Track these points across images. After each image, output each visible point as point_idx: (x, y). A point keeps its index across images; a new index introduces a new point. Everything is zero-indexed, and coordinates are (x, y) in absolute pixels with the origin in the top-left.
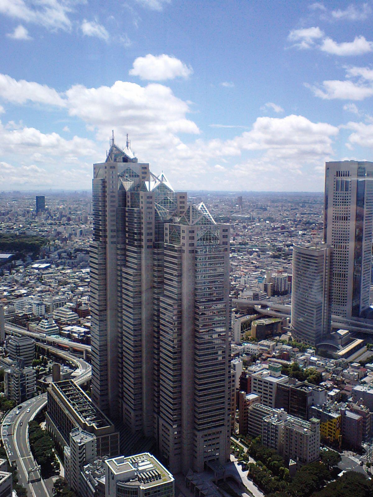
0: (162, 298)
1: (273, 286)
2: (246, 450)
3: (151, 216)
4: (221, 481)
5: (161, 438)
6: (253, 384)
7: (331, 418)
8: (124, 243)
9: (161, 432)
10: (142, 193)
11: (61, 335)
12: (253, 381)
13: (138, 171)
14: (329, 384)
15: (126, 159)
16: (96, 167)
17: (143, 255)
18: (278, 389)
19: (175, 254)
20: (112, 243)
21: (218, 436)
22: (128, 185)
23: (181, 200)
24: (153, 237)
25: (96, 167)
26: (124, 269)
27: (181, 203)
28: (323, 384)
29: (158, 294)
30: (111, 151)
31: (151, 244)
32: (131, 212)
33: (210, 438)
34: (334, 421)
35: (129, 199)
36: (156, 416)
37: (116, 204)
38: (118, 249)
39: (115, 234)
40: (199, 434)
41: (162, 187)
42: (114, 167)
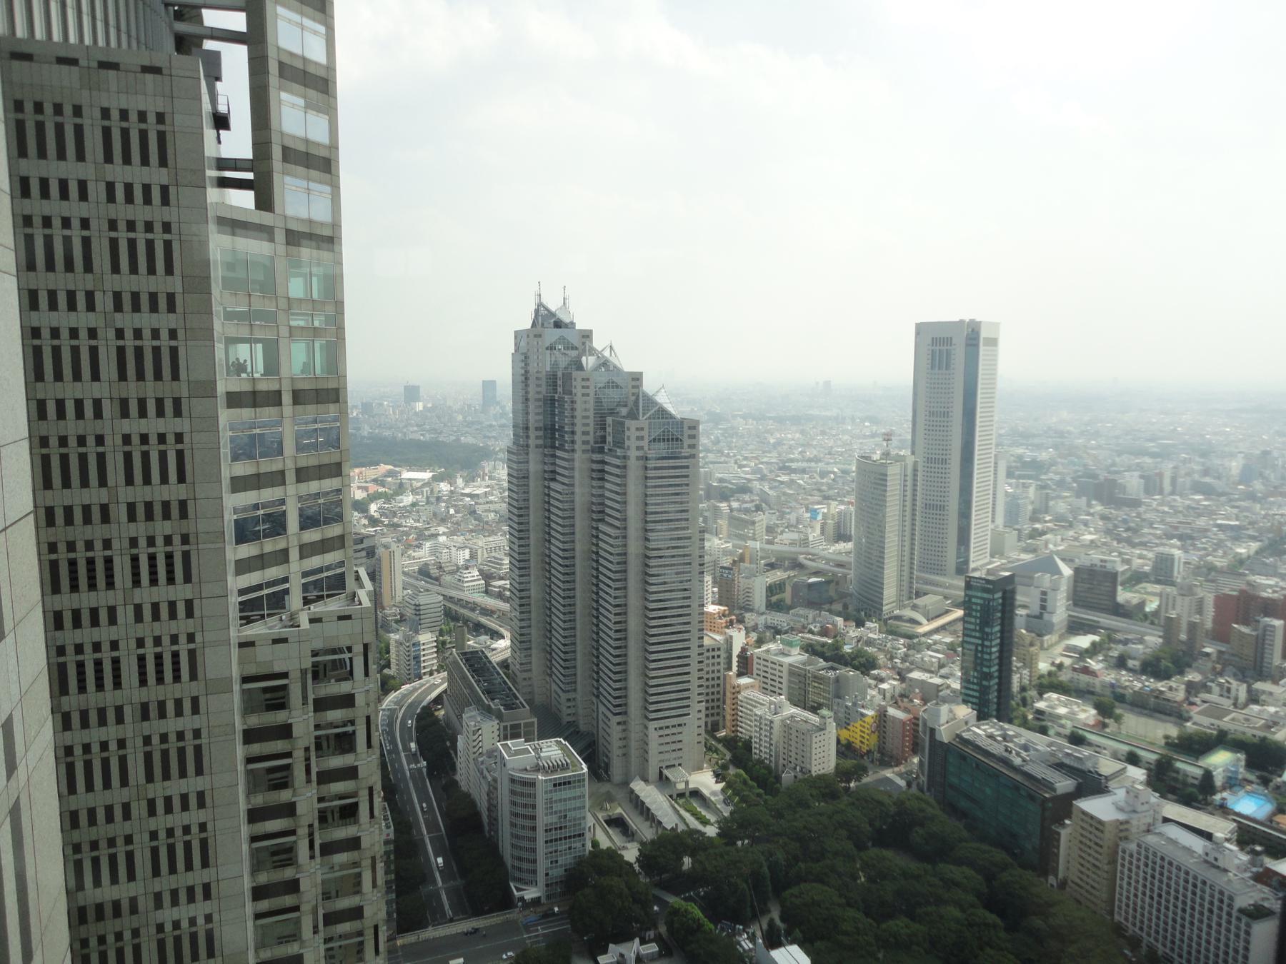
0: (602, 527)
1: (838, 526)
2: (728, 756)
3: (587, 406)
4: (681, 795)
5: (601, 732)
6: (755, 666)
7: (863, 715)
8: (553, 447)
9: (601, 724)
10: (577, 374)
11: (487, 592)
12: (755, 660)
13: (575, 341)
14: (883, 673)
15: (558, 324)
16: (518, 335)
17: (577, 464)
18: (791, 673)
19: (618, 462)
20: (537, 447)
21: (680, 729)
22: (563, 362)
23: (634, 383)
24: (591, 438)
25: (518, 335)
26: (553, 485)
27: (634, 387)
28: (875, 672)
29: (600, 520)
30: (537, 311)
31: (588, 447)
32: (561, 400)
33: (668, 731)
34: (866, 719)
35: (560, 382)
36: (594, 700)
37: (543, 389)
38: (545, 455)
39: (541, 433)
40: (652, 725)
41: (605, 364)
42: (540, 336)
